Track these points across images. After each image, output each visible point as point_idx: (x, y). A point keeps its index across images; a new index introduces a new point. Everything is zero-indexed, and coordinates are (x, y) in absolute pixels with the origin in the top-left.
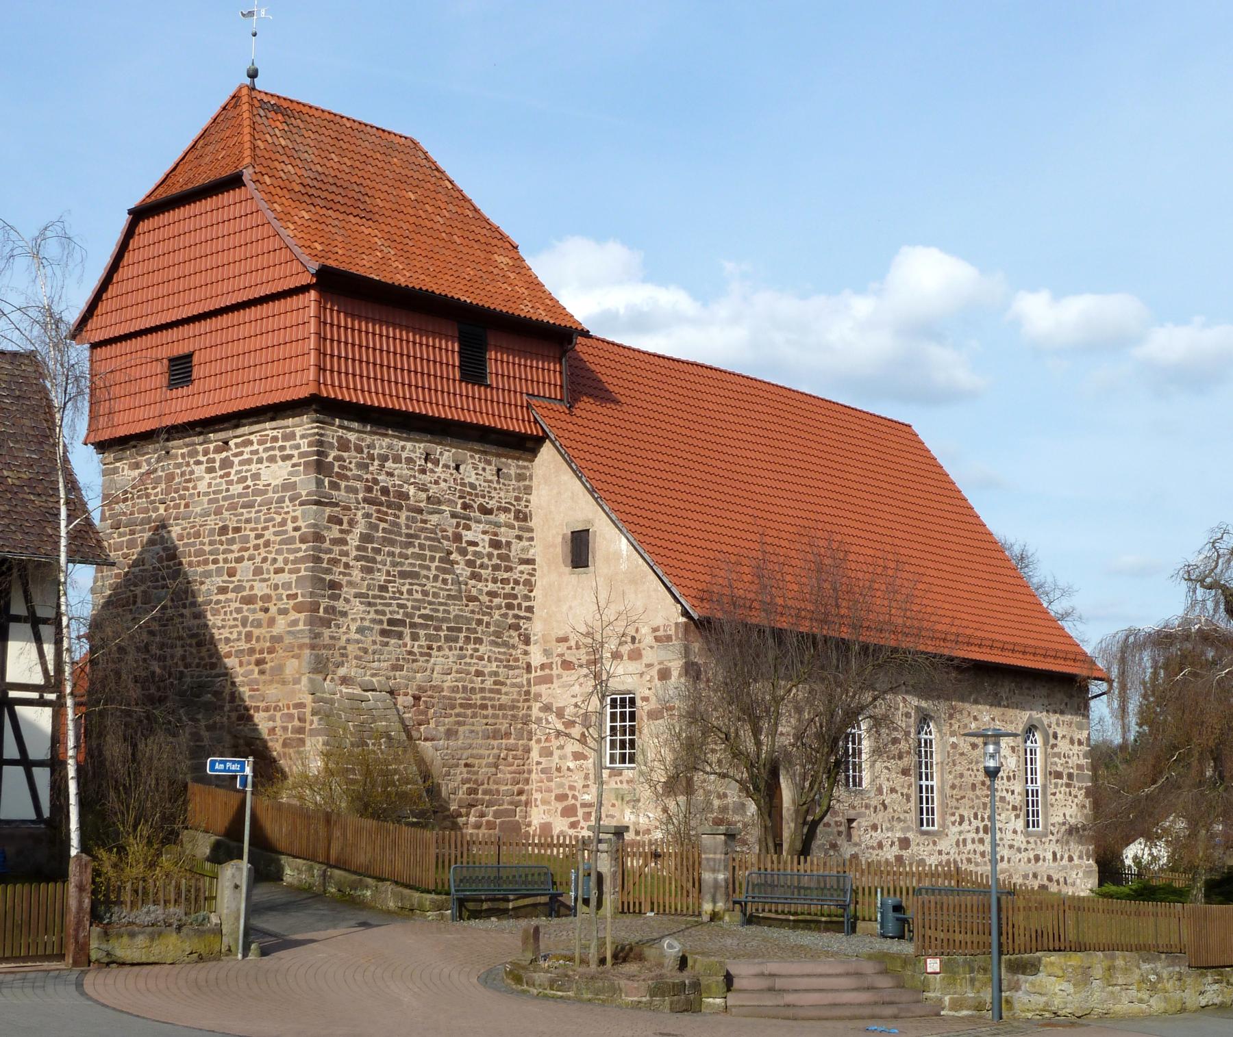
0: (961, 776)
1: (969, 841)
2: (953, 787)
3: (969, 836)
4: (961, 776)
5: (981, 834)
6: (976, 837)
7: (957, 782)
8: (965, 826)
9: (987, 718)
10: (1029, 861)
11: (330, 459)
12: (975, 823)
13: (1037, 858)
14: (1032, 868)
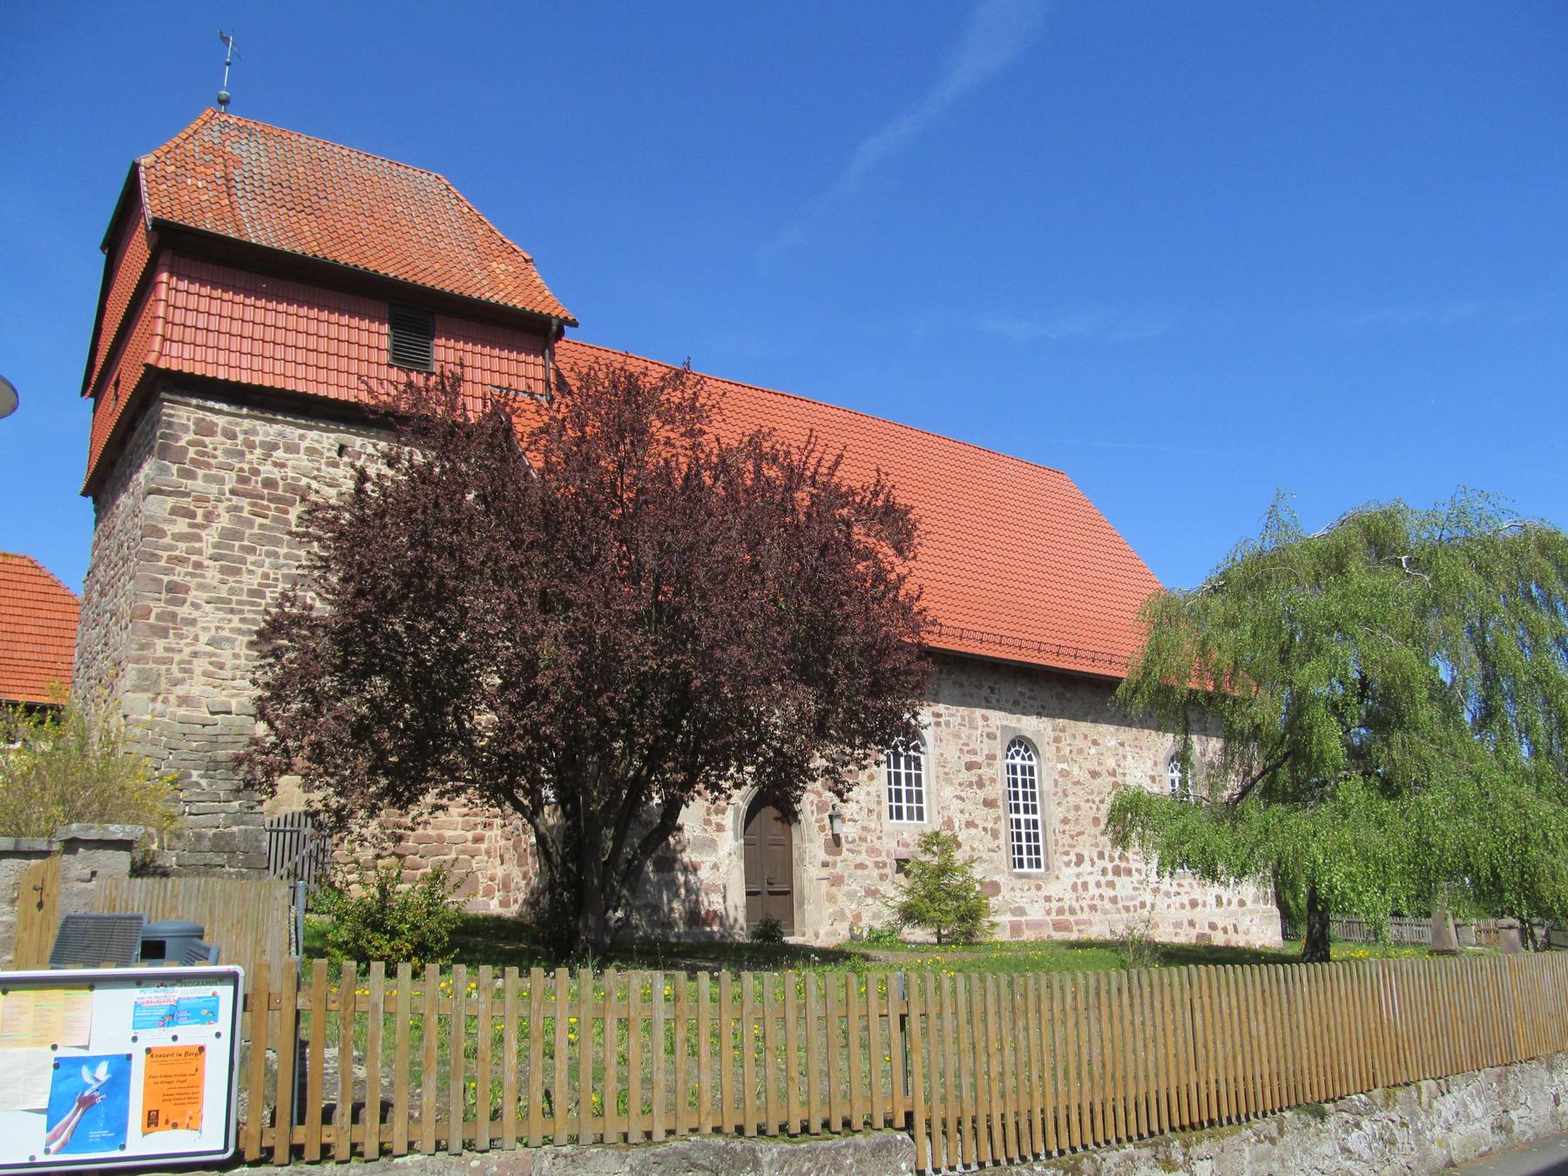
0: (1077, 808)
1: (1091, 885)
2: (1065, 821)
3: (1091, 880)
4: (1077, 808)
5: (1110, 877)
6: (1103, 880)
7: (1071, 815)
8: (1086, 866)
9: (1113, 743)
10: (1183, 906)
11: (182, 443)
12: (1100, 864)
13: (1194, 904)
14: (1187, 914)
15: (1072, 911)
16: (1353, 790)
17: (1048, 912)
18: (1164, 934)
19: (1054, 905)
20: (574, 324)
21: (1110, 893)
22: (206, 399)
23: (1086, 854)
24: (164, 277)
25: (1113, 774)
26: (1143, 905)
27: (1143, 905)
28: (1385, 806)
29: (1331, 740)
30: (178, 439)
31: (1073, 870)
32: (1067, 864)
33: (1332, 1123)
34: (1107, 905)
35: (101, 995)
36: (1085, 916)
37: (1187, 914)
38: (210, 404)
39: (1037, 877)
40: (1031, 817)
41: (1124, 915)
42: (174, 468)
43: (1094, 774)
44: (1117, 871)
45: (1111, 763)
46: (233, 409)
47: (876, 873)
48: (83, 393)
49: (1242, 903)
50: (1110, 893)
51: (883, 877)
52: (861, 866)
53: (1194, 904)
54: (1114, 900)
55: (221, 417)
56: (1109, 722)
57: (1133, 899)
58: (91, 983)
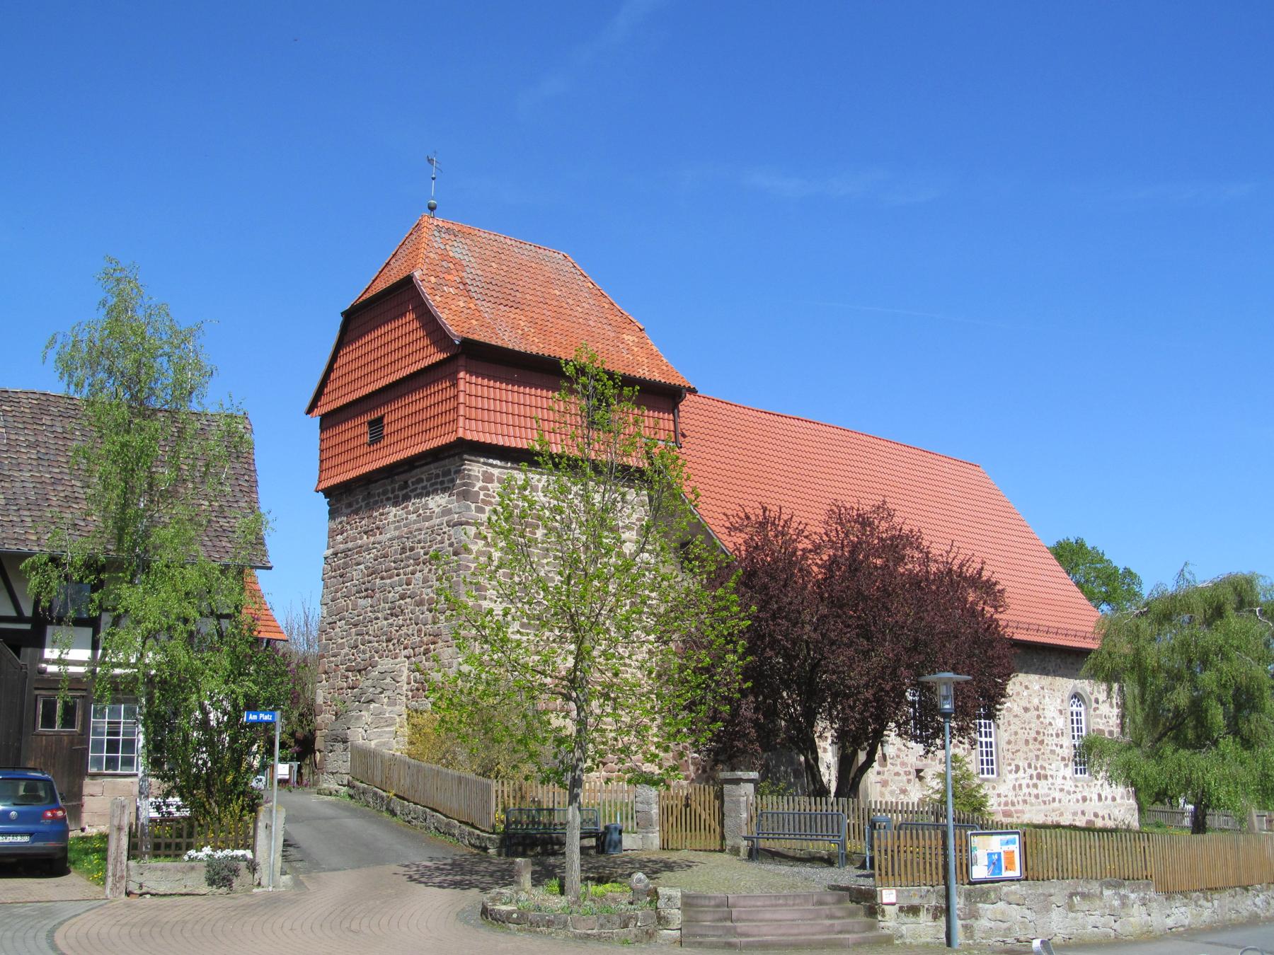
0: (1016, 733)
1: (1024, 786)
2: (1009, 742)
3: (1024, 782)
4: (1016, 733)
5: (1035, 780)
6: (1031, 783)
7: (1012, 738)
8: (1021, 772)
9: (1037, 687)
10: (1078, 801)
11: (476, 489)
12: (1029, 771)
13: (1084, 799)
14: (1081, 806)
15: (1013, 804)
16: (1228, 745)
17: (999, 805)
18: (1035, 822)
19: (1003, 800)
20: (693, 391)
21: (1034, 791)
22: (488, 458)
23: (1021, 764)
24: (462, 375)
25: (1037, 709)
26: (1054, 800)
27: (1054, 800)
28: (1246, 754)
29: (1217, 716)
30: (474, 486)
31: (1013, 776)
32: (1010, 772)
33: (1250, 893)
34: (1033, 800)
35: (994, 837)
36: (1019, 807)
37: (1081, 806)
38: (491, 461)
39: (993, 781)
40: (988, 740)
41: (1043, 807)
42: (473, 506)
43: (1026, 710)
44: (1039, 776)
45: (1036, 701)
46: (503, 464)
47: (905, 778)
48: (310, 411)
49: (1114, 799)
50: (1034, 791)
51: (909, 781)
52: (897, 774)
53: (1084, 799)
54: (1037, 796)
55: (498, 470)
56: (1035, 673)
57: (1048, 795)
58: (992, 834)
